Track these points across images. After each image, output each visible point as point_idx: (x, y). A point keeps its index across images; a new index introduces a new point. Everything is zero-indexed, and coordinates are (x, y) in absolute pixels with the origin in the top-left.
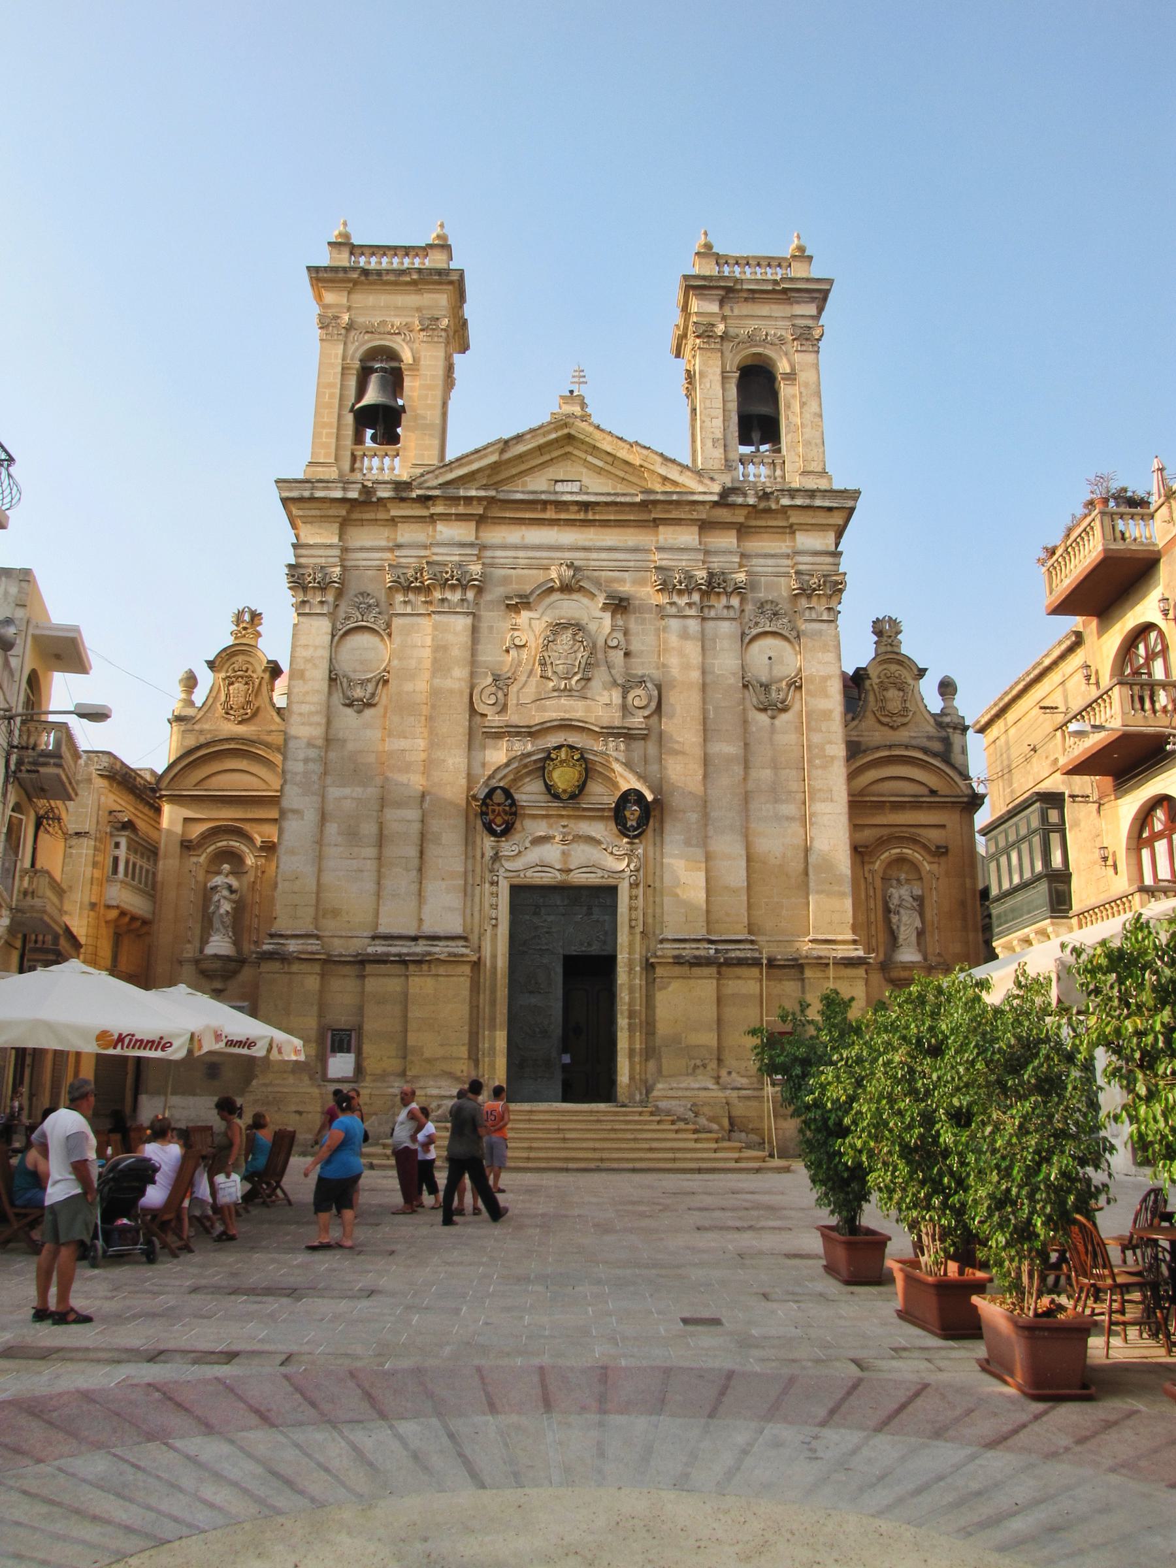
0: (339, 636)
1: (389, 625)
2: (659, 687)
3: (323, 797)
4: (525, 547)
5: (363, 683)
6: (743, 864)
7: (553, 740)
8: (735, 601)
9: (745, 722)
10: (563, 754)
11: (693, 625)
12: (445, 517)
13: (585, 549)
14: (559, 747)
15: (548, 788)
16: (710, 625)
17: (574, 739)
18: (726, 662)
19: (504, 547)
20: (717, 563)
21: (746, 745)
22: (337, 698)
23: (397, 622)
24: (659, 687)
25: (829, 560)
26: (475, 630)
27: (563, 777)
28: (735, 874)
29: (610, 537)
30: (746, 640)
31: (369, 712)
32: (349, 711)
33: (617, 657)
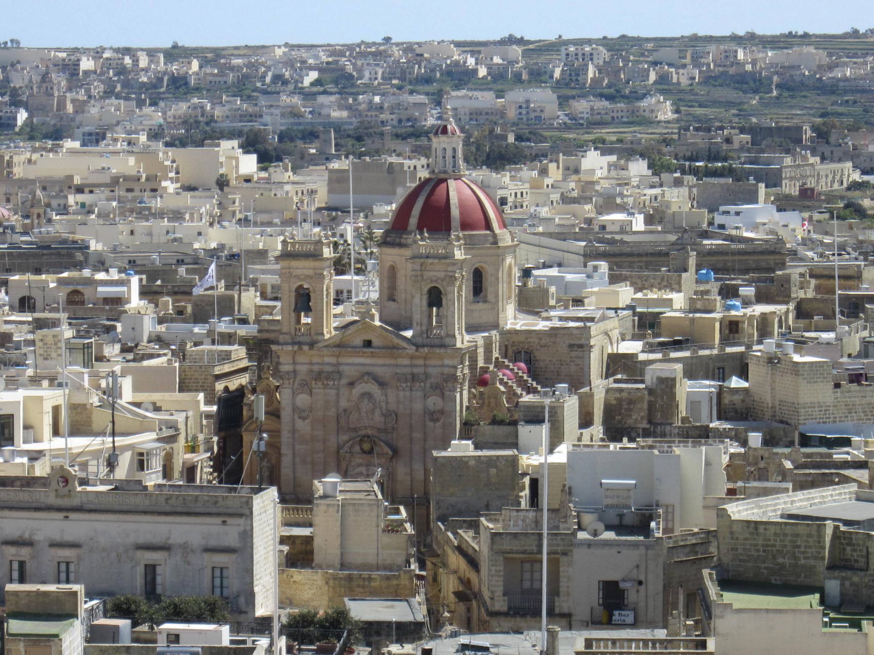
0: (294, 394)
1: (311, 391)
2: (396, 415)
3: (294, 449)
4: (353, 364)
5: (304, 411)
6: (423, 472)
7: (363, 432)
8: (422, 384)
9: (425, 425)
10: (366, 439)
11: (408, 393)
12: (328, 356)
13: (373, 365)
14: (364, 437)
15: (362, 449)
16: (414, 393)
17: (370, 432)
18: (418, 406)
19: (348, 364)
20: (415, 370)
21: (425, 433)
22: (296, 416)
23: (314, 391)
24: (396, 415)
25: (453, 370)
26: (338, 395)
27: (366, 446)
28: (420, 475)
29: (381, 361)
30: (425, 397)
31: (306, 421)
32: (300, 421)
33: (383, 405)
